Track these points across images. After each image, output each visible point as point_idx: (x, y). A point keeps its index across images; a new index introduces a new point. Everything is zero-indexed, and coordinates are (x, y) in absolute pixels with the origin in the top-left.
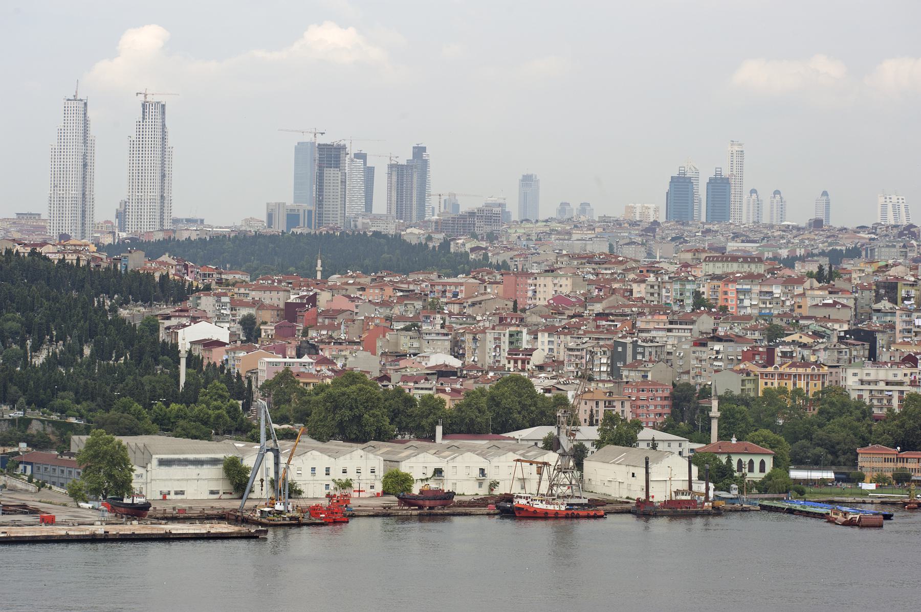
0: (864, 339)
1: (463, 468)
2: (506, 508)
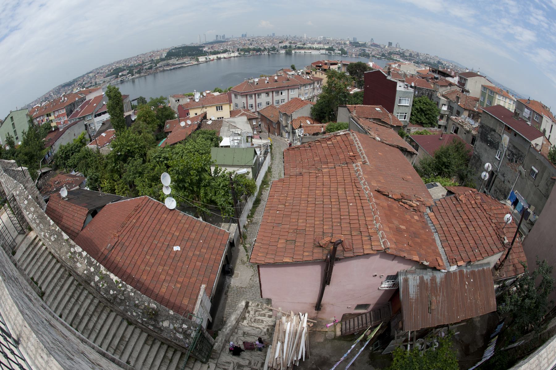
0: (251, 44)
1: (222, 56)
2: (225, 58)
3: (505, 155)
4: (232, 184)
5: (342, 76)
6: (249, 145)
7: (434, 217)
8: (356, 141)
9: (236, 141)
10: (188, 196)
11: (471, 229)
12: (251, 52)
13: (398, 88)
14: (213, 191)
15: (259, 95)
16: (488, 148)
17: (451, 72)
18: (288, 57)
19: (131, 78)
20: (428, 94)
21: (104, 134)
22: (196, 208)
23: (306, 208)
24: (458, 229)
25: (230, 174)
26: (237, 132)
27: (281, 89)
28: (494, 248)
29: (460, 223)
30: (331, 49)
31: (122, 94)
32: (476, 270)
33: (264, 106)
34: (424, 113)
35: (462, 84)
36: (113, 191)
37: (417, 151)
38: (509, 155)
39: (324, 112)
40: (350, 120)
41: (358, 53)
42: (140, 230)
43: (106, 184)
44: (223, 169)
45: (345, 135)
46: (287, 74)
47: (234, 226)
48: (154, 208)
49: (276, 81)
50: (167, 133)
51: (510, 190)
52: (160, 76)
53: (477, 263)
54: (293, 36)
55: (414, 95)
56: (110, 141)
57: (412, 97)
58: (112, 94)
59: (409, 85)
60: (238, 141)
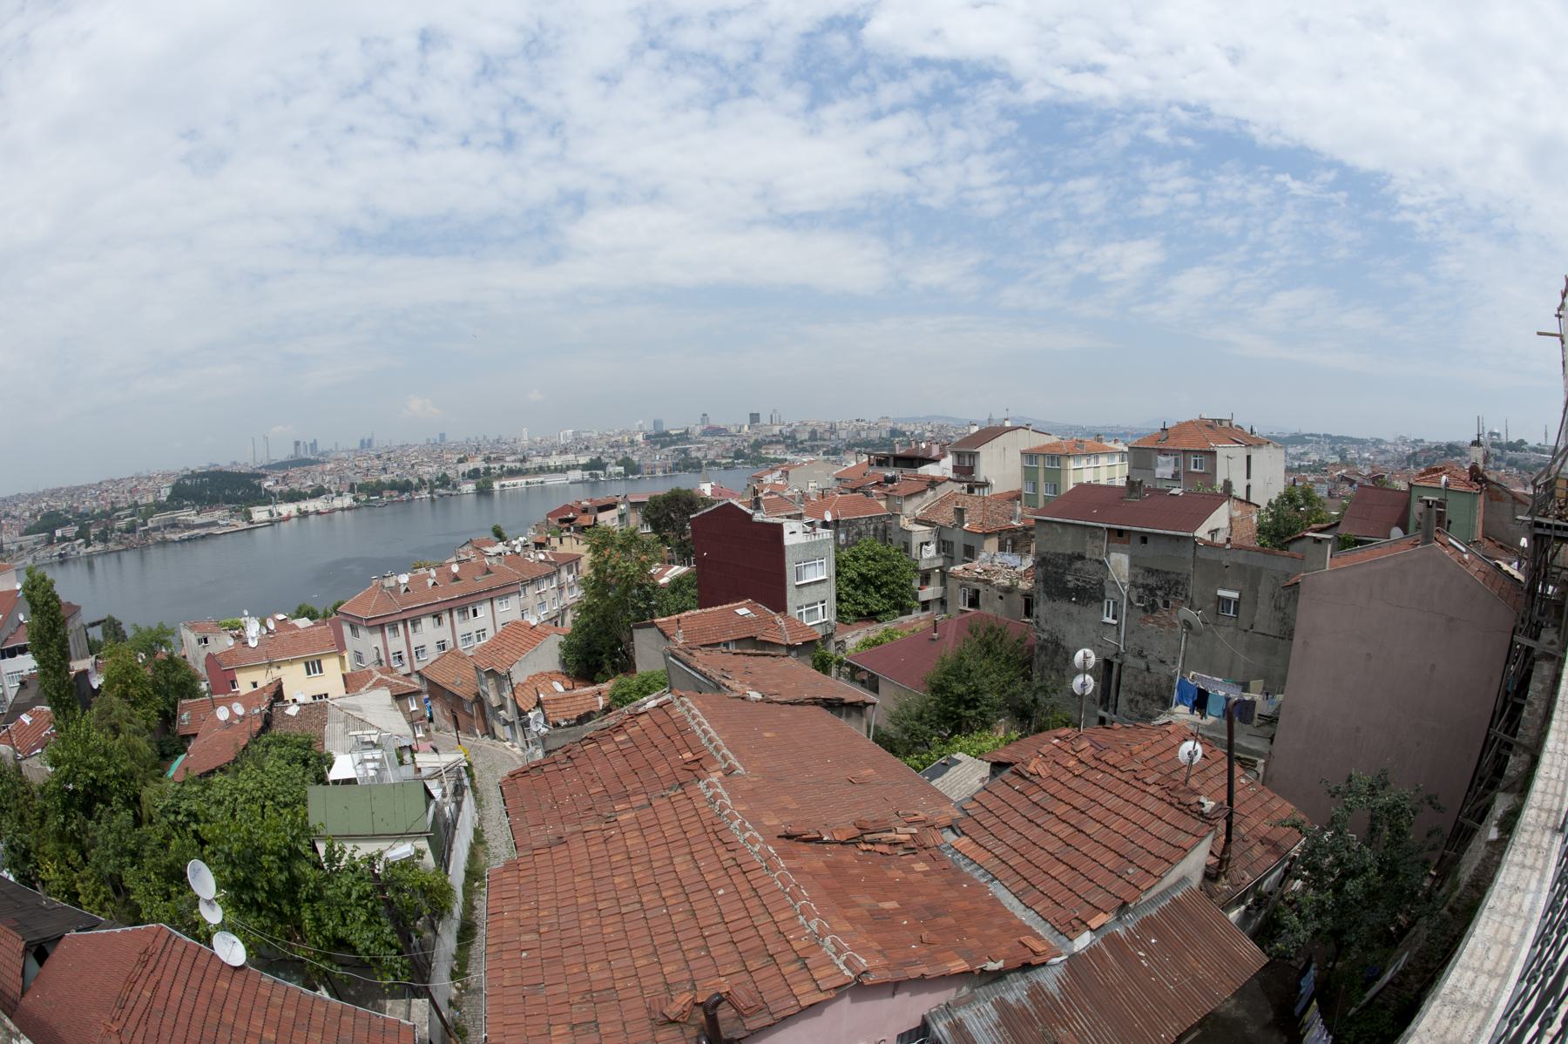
1: (310, 505)
2: (318, 513)
3: (1130, 603)
4: (382, 890)
5: (631, 540)
6: (407, 772)
7: (973, 846)
8: (694, 717)
9: (370, 765)
10: (272, 930)
11: (1092, 827)
12: (386, 493)
13: (788, 540)
14: (335, 912)
15: (416, 622)
16: (1074, 609)
17: (929, 449)
18: (484, 500)
19: (83, 551)
20: (876, 529)
21: (26, 719)
22: (301, 961)
23: (598, 929)
24: (1054, 846)
25: (371, 860)
26: (367, 739)
27: (470, 600)
28: (1181, 838)
29: (1054, 830)
30: (596, 465)
31: (64, 598)
32: (1154, 912)
33: (432, 653)
34: (873, 585)
35: (965, 470)
36: (73, 897)
37: (876, 690)
38: (1140, 599)
39: (596, 653)
40: (667, 661)
41: (670, 462)
42: (169, 1021)
43: (50, 871)
44: (349, 847)
45: (660, 706)
46: (484, 554)
47: (420, 1006)
48: (188, 960)
49: (456, 578)
50: (187, 738)
51: (1171, 679)
52: (155, 554)
53: (1145, 898)
54: (492, 437)
55: (837, 545)
56: (43, 744)
57: (832, 552)
58: (38, 596)
59: (819, 522)
60: (377, 765)
